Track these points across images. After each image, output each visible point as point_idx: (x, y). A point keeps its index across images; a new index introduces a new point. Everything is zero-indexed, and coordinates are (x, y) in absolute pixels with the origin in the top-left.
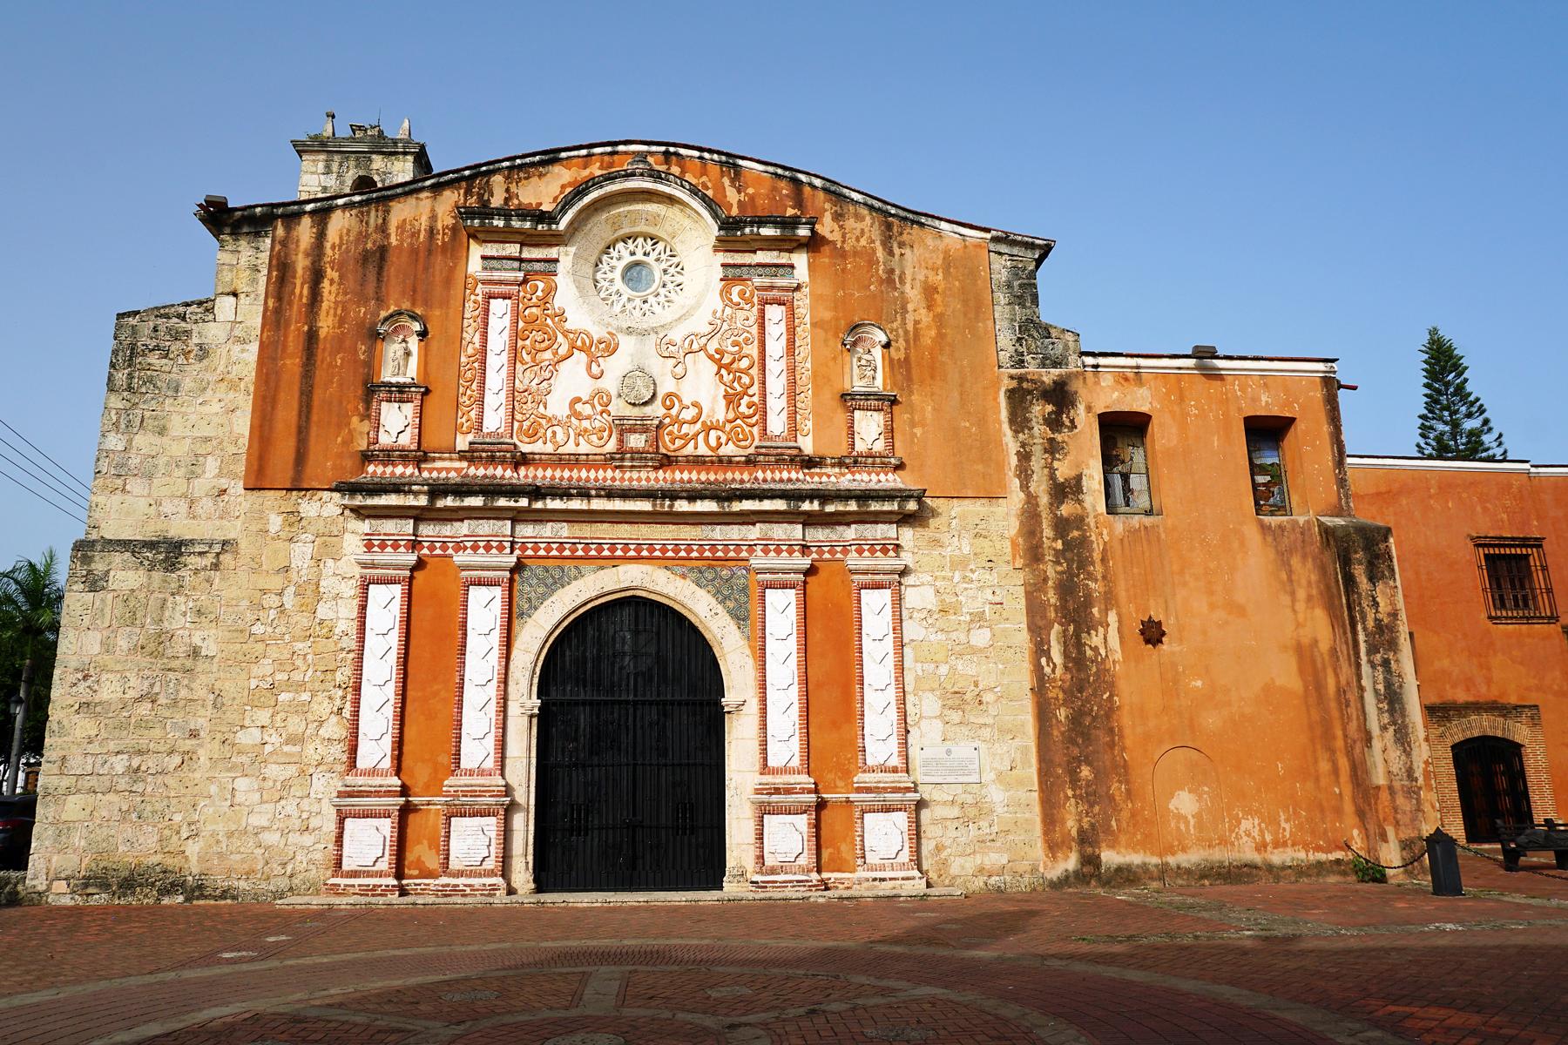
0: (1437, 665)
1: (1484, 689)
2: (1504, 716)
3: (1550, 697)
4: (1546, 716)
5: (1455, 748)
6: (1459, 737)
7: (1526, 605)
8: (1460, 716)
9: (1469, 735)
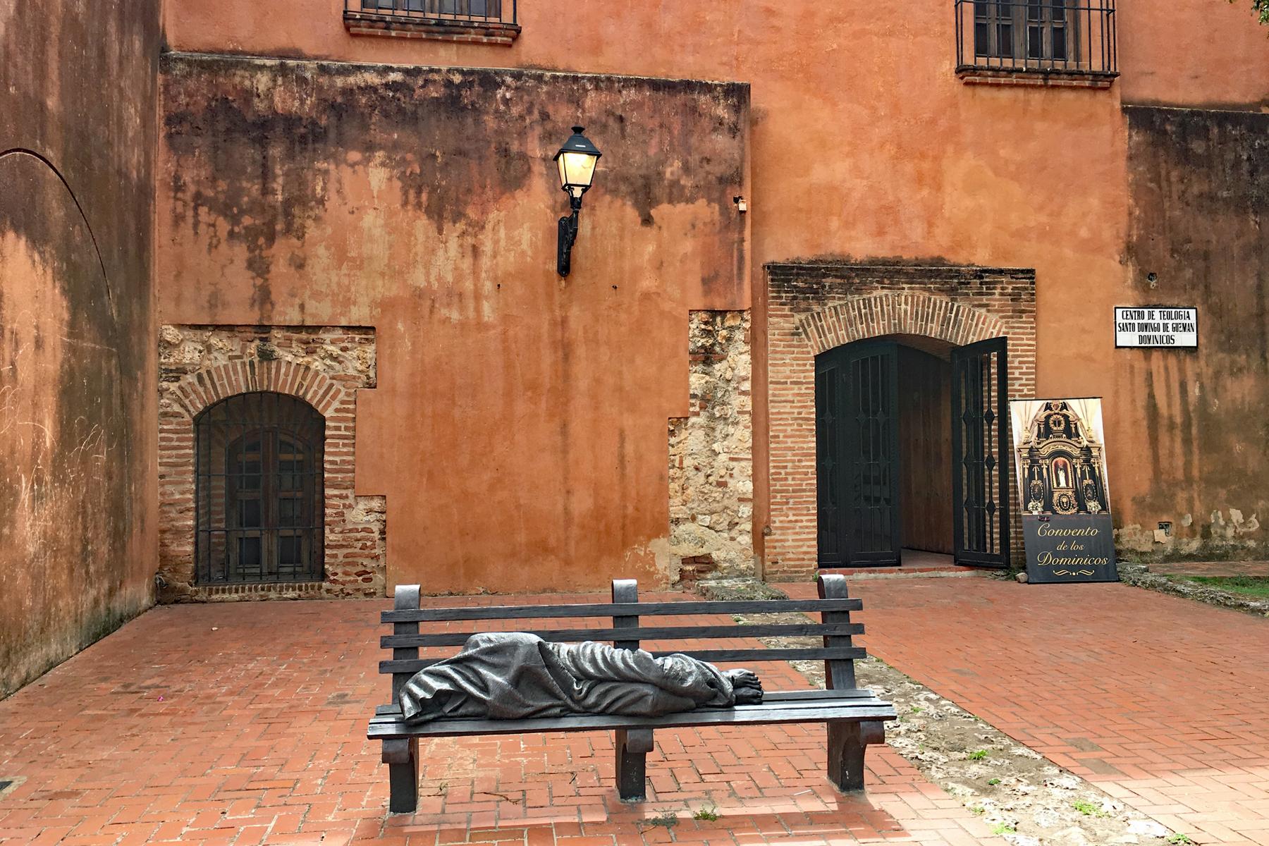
0: (819, 174)
1: (916, 232)
2: (952, 292)
3: (1068, 252)
4: (1050, 294)
5: (820, 360)
6: (837, 336)
7: (1059, 53)
8: (848, 289)
9: (861, 332)
